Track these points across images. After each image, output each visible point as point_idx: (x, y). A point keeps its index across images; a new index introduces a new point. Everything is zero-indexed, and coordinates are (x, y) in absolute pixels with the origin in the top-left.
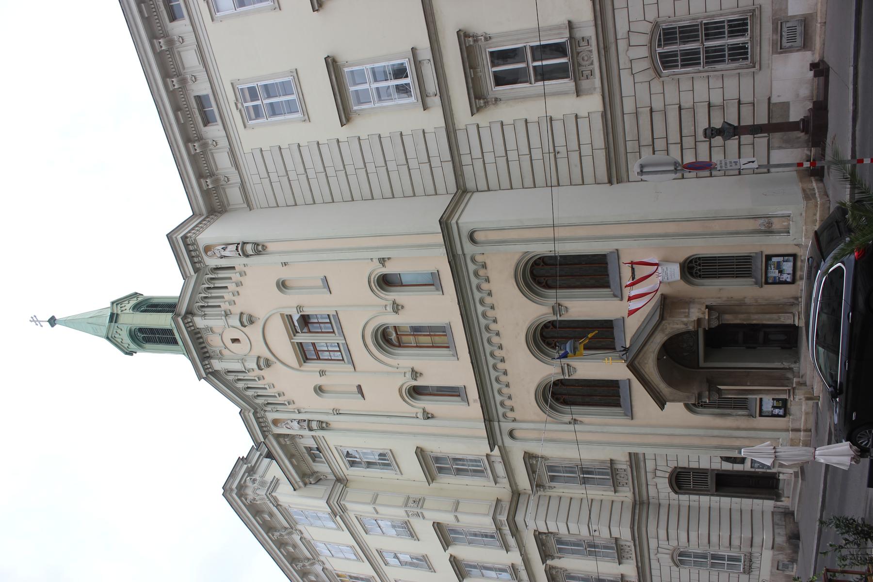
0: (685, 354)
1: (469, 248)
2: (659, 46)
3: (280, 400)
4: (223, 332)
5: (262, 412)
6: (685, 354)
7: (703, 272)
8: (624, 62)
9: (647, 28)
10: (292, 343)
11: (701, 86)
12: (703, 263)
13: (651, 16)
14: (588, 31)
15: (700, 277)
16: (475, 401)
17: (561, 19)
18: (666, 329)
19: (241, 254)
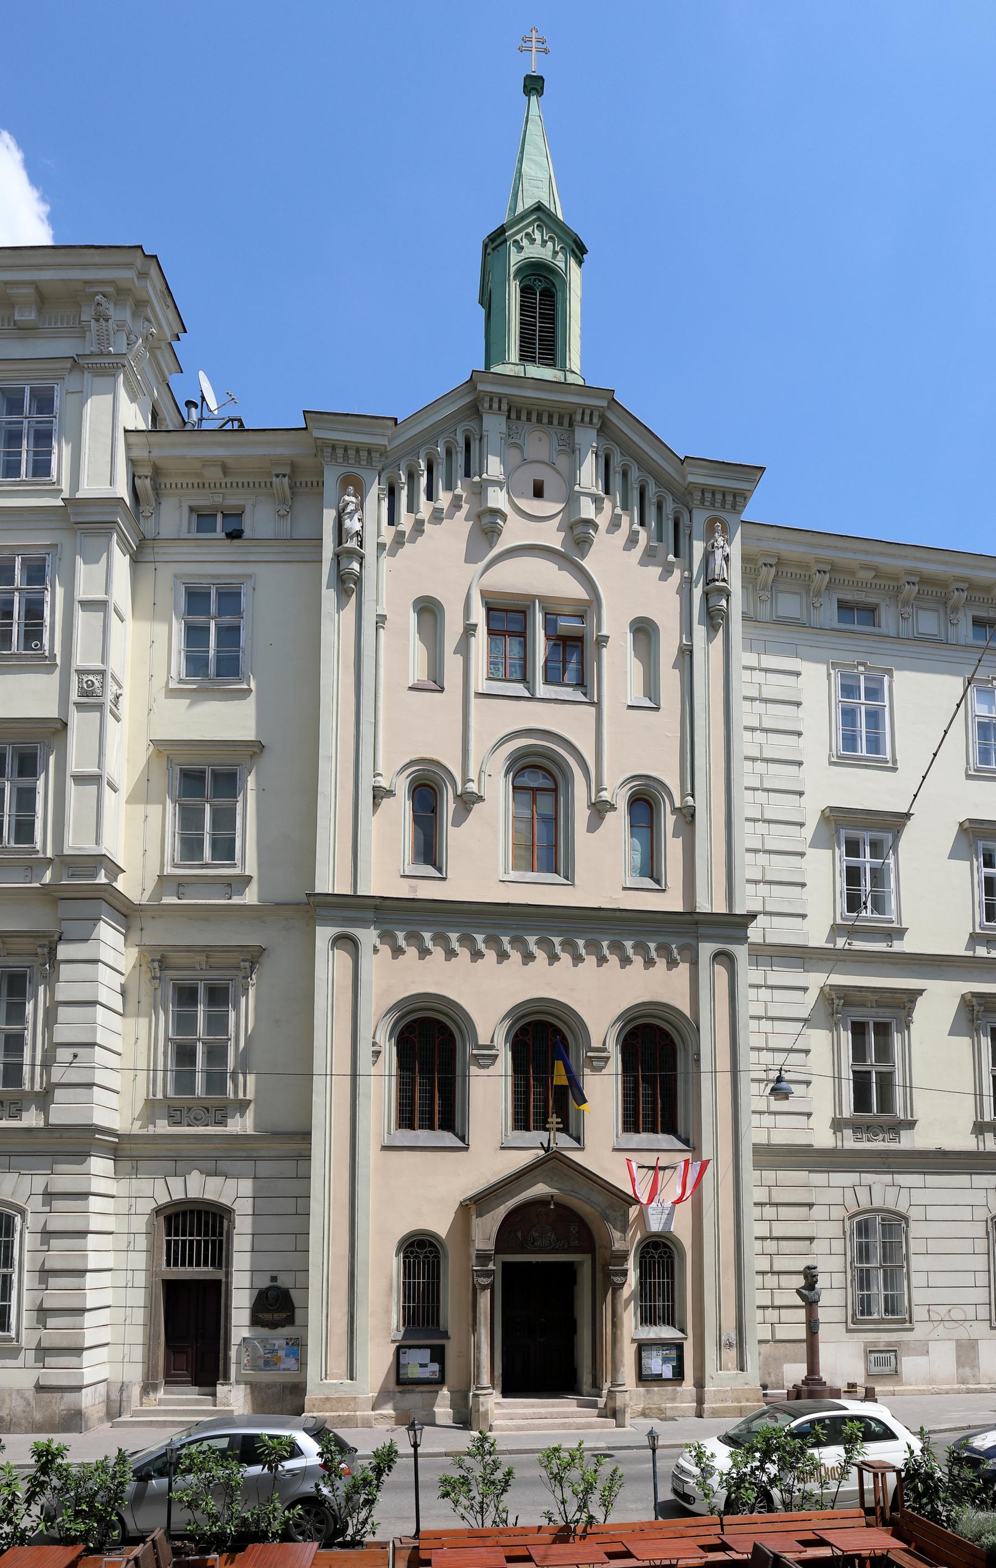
0: (519, 1234)
1: (706, 949)
2: (883, 1219)
3: (406, 521)
4: (558, 472)
5: (380, 468)
6: (519, 1234)
7: (667, 1261)
8: (868, 1178)
9: (902, 1208)
10: (532, 598)
11: (836, 1263)
12: (663, 1261)
13: (914, 1213)
14: (909, 1141)
15: (640, 1258)
16: (414, 889)
17: (921, 1111)
18: (614, 1211)
19: (712, 585)
